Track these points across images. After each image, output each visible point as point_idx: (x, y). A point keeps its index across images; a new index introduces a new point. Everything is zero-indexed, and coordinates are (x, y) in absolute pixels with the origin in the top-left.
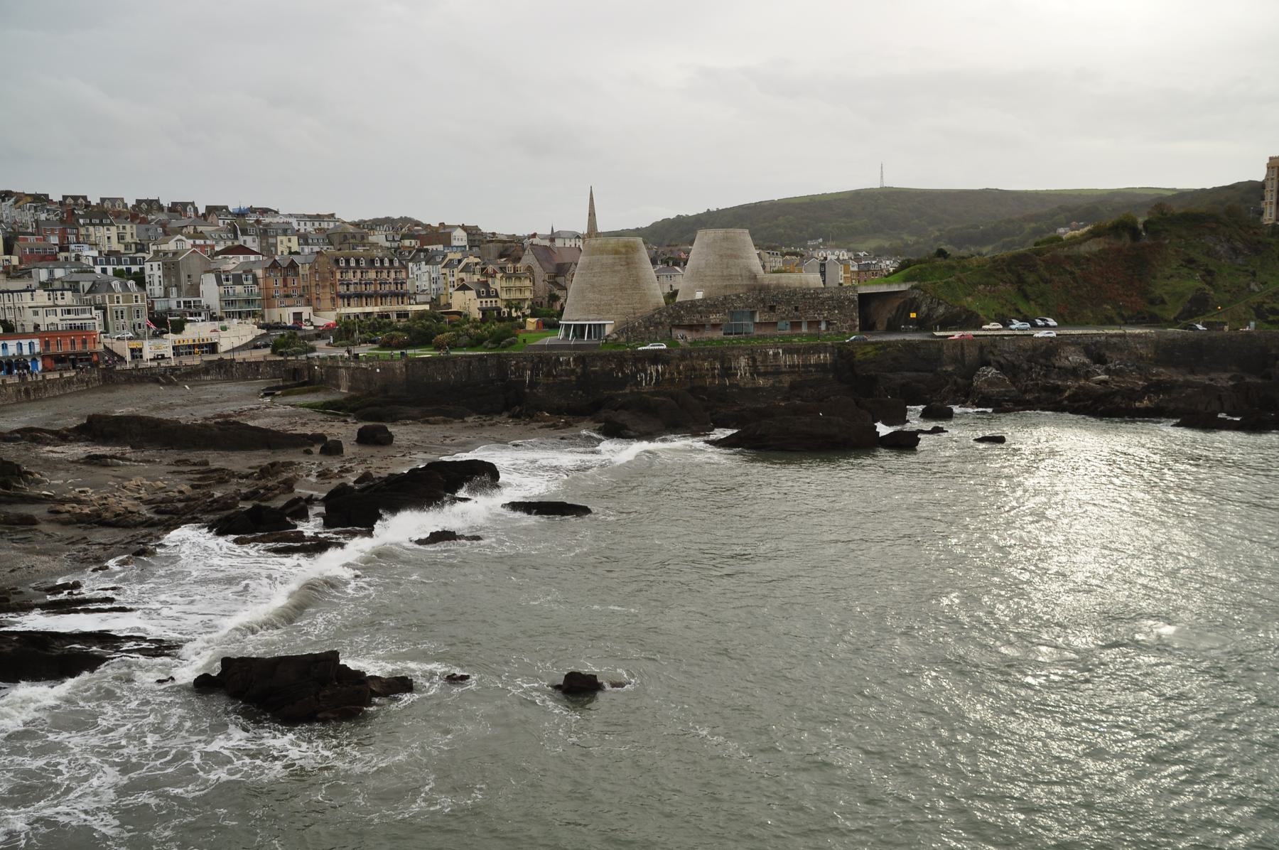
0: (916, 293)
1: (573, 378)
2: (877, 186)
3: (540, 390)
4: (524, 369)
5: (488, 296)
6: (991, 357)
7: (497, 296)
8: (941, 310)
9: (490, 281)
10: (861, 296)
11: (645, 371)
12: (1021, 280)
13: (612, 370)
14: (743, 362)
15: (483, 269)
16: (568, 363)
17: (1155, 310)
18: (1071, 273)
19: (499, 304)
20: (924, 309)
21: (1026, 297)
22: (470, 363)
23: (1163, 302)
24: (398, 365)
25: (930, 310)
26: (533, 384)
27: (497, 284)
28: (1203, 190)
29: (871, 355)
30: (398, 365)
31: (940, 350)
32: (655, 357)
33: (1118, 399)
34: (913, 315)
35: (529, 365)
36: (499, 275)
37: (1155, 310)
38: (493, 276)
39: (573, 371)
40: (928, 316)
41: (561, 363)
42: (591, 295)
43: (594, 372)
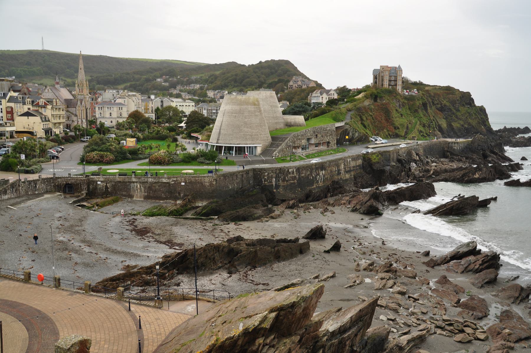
1: (296, 181)
2: (40, 48)
3: (281, 190)
4: (272, 177)
5: (46, 121)
6: (400, 158)
7: (49, 121)
8: (357, 135)
9: (42, 111)
10: (337, 128)
11: (319, 174)
12: (362, 120)
13: (309, 175)
14: (342, 166)
15: (33, 102)
16: (293, 173)
17: (397, 131)
18: (371, 116)
19: (51, 126)
20: (351, 134)
21: (365, 126)
22: (242, 175)
23: (398, 128)
24: (207, 180)
25: (353, 134)
26: (277, 187)
27: (48, 112)
28: (216, 64)
29: (377, 160)
30: (207, 180)
31: (390, 155)
32: (321, 166)
33: (471, 175)
34: (347, 137)
35: (274, 176)
36: (49, 107)
37: (397, 131)
38: (44, 106)
39: (295, 177)
40: (353, 138)
41: (290, 173)
42: (246, 129)
43: (303, 177)
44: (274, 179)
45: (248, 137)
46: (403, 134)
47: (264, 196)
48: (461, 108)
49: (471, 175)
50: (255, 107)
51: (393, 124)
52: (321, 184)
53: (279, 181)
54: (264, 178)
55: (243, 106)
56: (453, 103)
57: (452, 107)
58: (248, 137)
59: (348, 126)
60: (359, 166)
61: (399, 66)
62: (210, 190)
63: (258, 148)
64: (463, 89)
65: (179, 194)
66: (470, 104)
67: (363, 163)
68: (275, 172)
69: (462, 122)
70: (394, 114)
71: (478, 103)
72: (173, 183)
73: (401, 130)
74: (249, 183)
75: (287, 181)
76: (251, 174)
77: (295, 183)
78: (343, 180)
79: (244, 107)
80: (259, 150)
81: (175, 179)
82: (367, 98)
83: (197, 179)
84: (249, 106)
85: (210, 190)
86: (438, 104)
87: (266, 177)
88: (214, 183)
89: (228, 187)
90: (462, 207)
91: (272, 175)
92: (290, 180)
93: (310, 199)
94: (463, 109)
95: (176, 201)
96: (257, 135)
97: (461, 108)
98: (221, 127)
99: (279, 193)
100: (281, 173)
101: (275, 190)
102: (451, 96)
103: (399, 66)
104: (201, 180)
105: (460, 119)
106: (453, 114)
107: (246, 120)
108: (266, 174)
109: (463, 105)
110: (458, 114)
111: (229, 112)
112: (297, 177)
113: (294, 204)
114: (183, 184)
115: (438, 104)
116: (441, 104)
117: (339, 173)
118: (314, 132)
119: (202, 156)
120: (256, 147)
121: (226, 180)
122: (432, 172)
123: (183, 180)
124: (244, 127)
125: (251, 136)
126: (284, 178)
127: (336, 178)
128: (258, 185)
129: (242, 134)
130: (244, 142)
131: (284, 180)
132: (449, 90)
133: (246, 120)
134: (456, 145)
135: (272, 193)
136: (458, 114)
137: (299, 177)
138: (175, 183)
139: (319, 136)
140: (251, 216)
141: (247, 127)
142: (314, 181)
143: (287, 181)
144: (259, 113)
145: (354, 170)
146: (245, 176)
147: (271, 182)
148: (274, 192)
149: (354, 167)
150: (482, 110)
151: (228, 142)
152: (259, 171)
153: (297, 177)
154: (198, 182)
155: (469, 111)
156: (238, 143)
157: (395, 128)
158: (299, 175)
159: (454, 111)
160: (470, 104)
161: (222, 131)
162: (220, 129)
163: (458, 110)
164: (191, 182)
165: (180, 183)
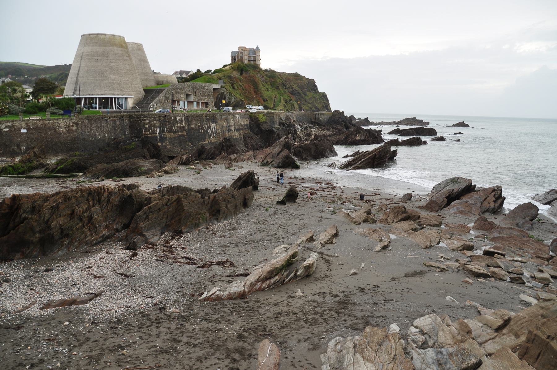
0: (223, 90)
4: (155, 127)
8: (233, 99)
10: (214, 89)
11: (210, 127)
18: (241, 86)
20: (227, 98)
22: (115, 121)
23: (267, 100)
25: (229, 99)
26: (162, 139)
29: (263, 120)
34: (224, 102)
35: (158, 124)
39: (184, 127)
41: (177, 122)
42: (112, 76)
43: (192, 128)
44: (158, 129)
45: (115, 86)
46: (272, 107)
47: (145, 151)
48: (308, 93)
49: (353, 137)
50: (123, 49)
51: (261, 96)
52: (213, 140)
53: (164, 131)
54: (144, 127)
55: (106, 48)
56: (302, 87)
57: (301, 92)
58: (115, 86)
59: (223, 89)
60: (246, 125)
61: (257, 48)
62: (69, 138)
63: (129, 100)
64: (309, 76)
65: (19, 147)
66: (315, 90)
67: (250, 123)
68: (158, 119)
69: (310, 106)
70: (261, 87)
71: (320, 90)
72: (7, 130)
73: (269, 102)
74: (125, 134)
75: (174, 132)
76: (126, 121)
77: (184, 135)
78: (234, 139)
79: (108, 48)
80: (130, 103)
81: (10, 124)
82: (235, 70)
83: (46, 122)
84: (115, 48)
85: (69, 138)
86: (289, 88)
87: (147, 126)
88: (74, 128)
89: (96, 137)
90: (384, 156)
91: (155, 124)
92: (178, 132)
93: (204, 156)
94: (310, 94)
95: (14, 158)
96: (127, 84)
97: (308, 93)
98: (78, 74)
99: (165, 147)
100: (166, 122)
101: (159, 144)
102: (299, 81)
103: (257, 48)
104: (53, 124)
105: (308, 103)
106: (302, 97)
107: (112, 65)
108: (147, 121)
109: (309, 91)
110: (306, 97)
111: (88, 55)
112: (186, 127)
113: (188, 159)
114: (24, 131)
115: (289, 88)
116: (292, 88)
117: (229, 131)
118: (193, 88)
119: (53, 105)
120: (126, 98)
121: (91, 125)
122: (313, 137)
123: (24, 125)
124: (110, 73)
125: (119, 84)
126: (171, 128)
127: (227, 135)
128: (137, 137)
129: (107, 81)
130: (110, 92)
131: (170, 131)
132: (296, 76)
133: (112, 65)
134: (322, 116)
135: (156, 147)
136: (306, 97)
137: (188, 128)
138: (10, 131)
139: (198, 94)
140: (136, 169)
141: (114, 74)
142: (204, 135)
143: (174, 132)
144: (128, 58)
145: (242, 129)
146: (118, 122)
147: (154, 133)
148: (159, 146)
149: (242, 126)
150: (324, 96)
151: (89, 92)
152: (138, 118)
153: (186, 127)
154: (49, 128)
155: (315, 96)
156: (102, 93)
157: (264, 100)
158: (188, 126)
159: (303, 95)
160: (315, 90)
161: (80, 80)
162: (77, 77)
163: (306, 95)
164: (37, 128)
165: (19, 130)
